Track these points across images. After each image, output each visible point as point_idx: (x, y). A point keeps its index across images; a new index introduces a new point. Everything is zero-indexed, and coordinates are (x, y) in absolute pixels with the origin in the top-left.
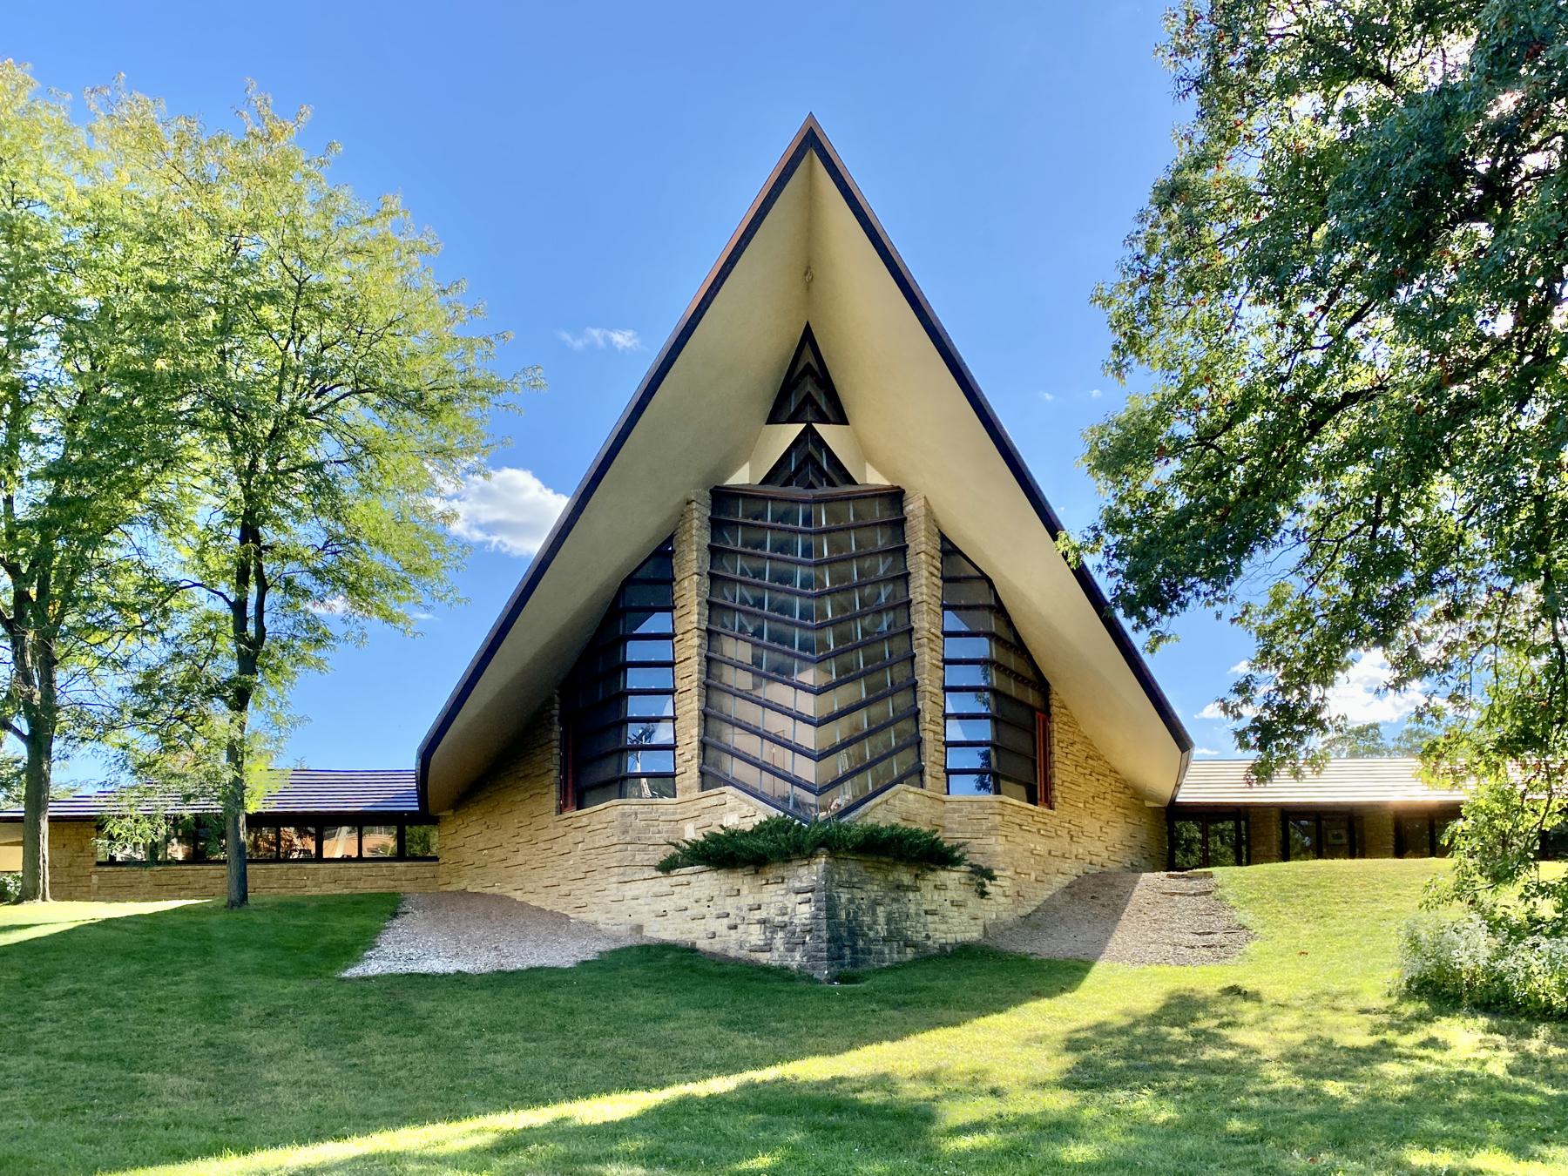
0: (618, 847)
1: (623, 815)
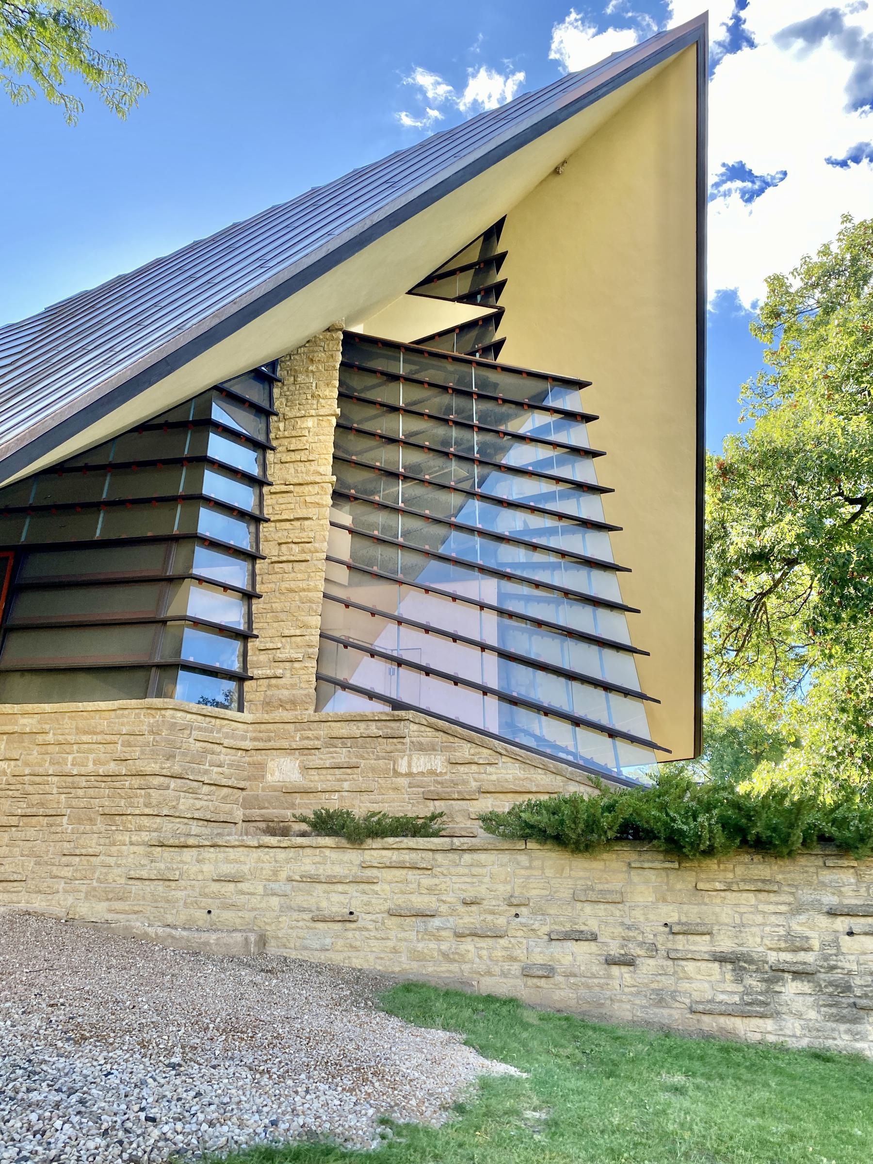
0: (157, 781)
1: (173, 726)
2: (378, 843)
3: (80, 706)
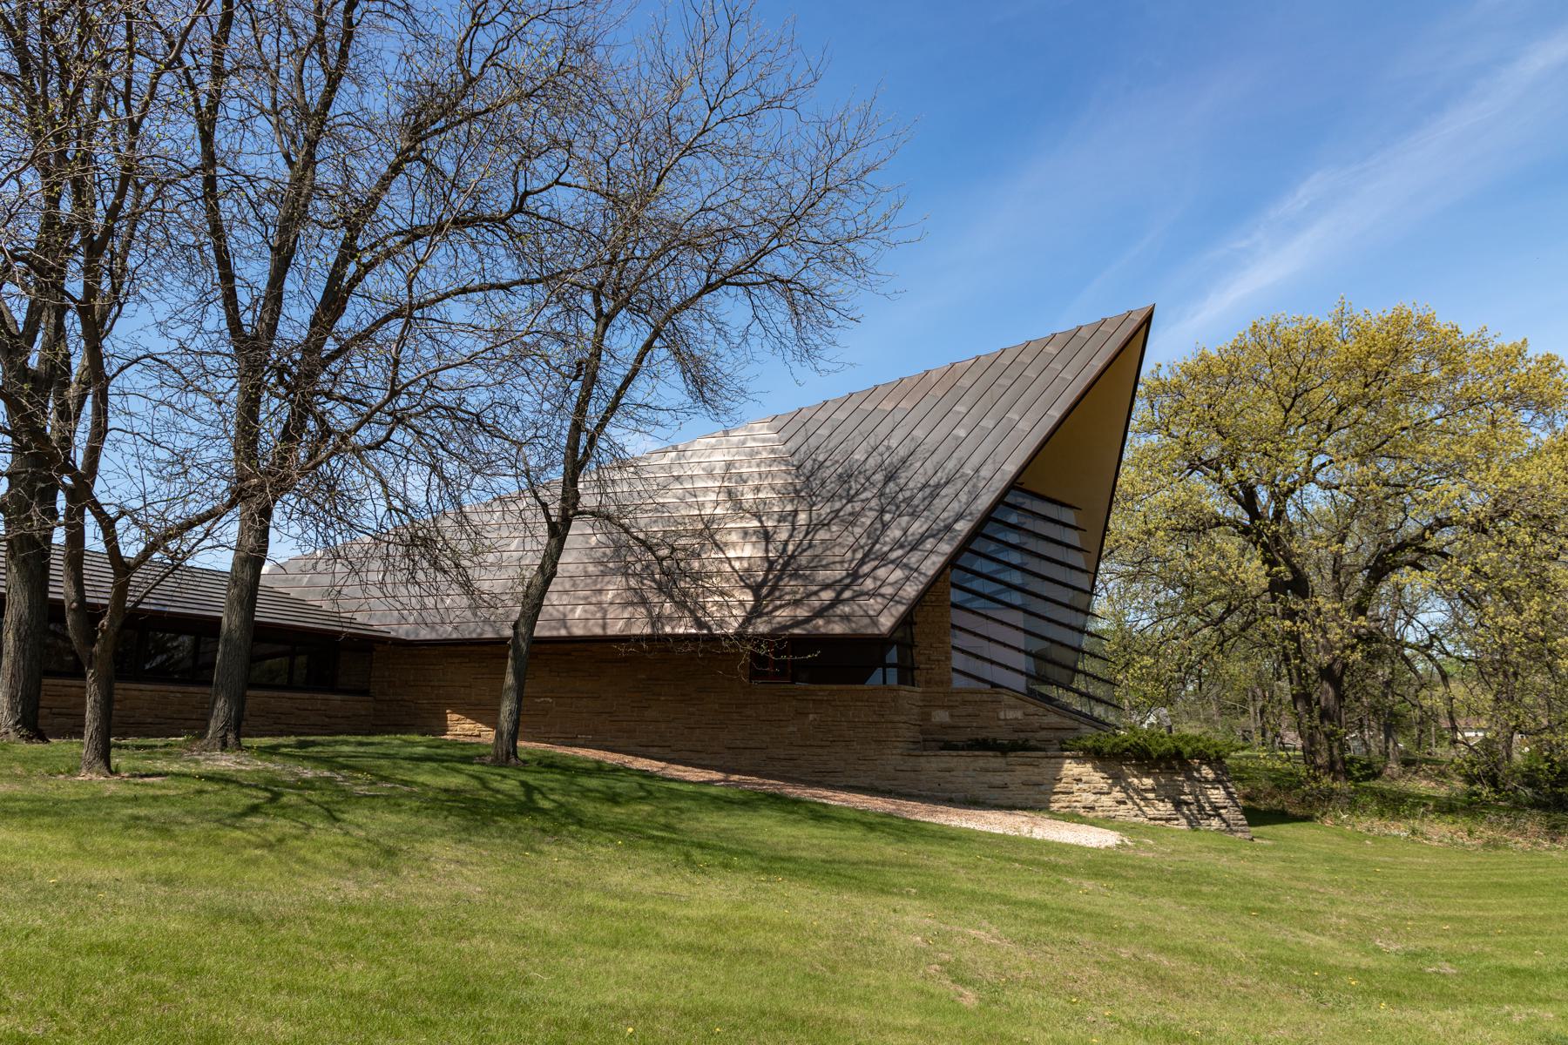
2: (1013, 754)
3: (853, 687)
